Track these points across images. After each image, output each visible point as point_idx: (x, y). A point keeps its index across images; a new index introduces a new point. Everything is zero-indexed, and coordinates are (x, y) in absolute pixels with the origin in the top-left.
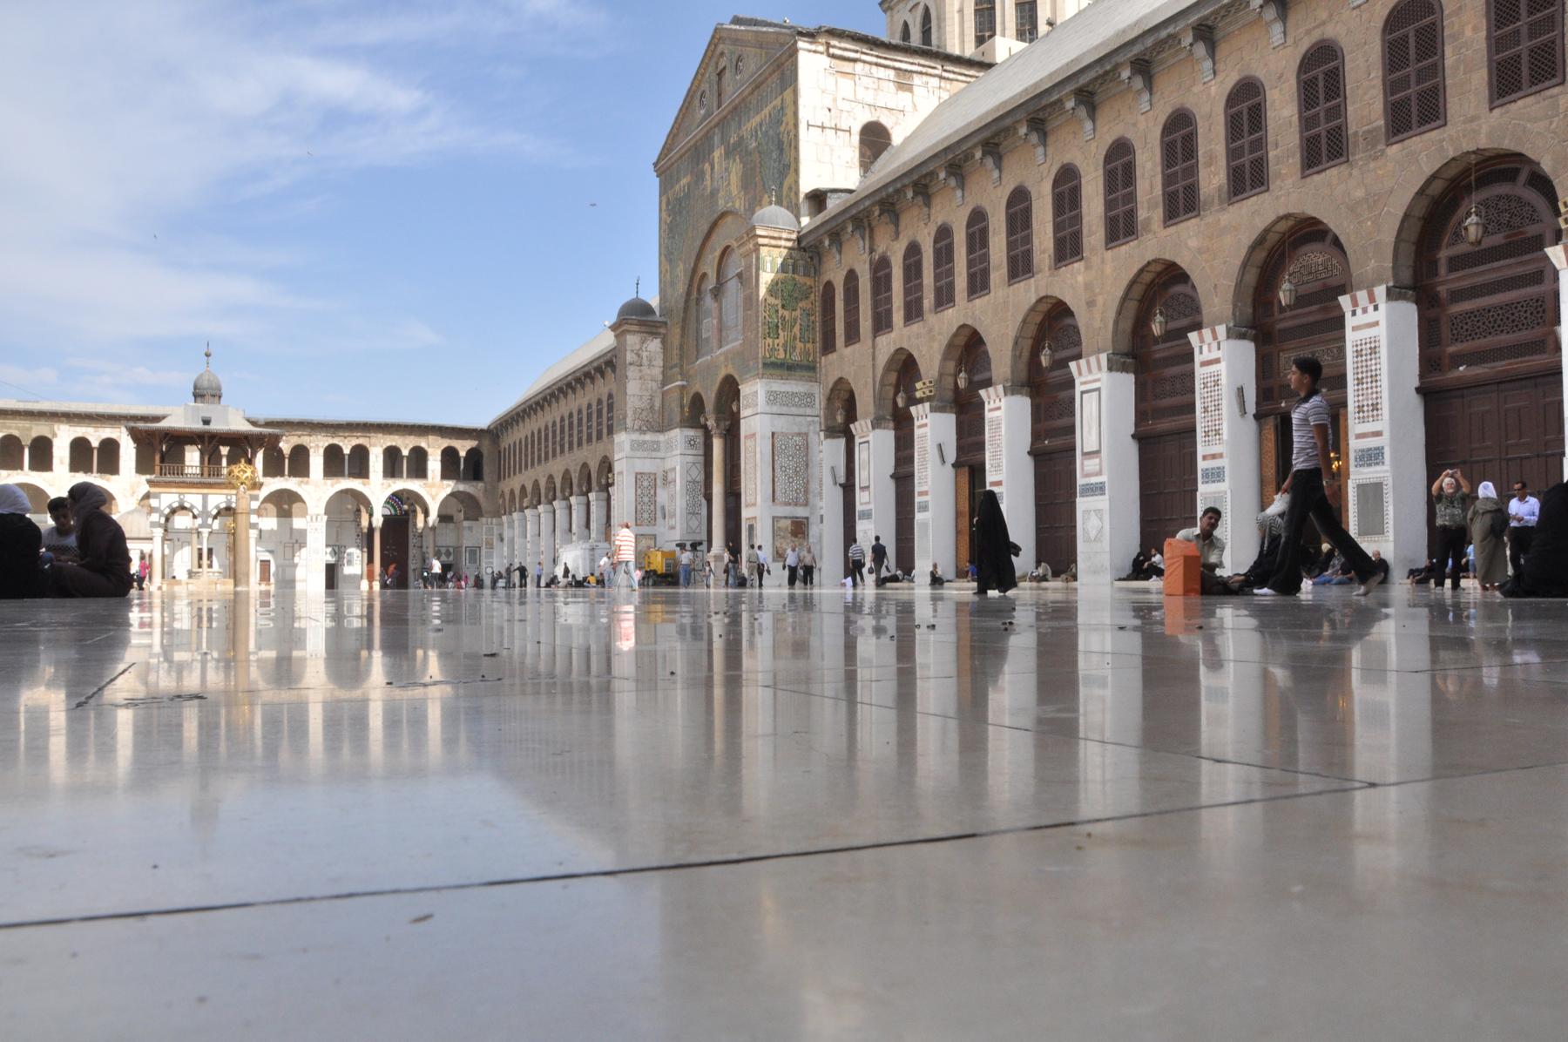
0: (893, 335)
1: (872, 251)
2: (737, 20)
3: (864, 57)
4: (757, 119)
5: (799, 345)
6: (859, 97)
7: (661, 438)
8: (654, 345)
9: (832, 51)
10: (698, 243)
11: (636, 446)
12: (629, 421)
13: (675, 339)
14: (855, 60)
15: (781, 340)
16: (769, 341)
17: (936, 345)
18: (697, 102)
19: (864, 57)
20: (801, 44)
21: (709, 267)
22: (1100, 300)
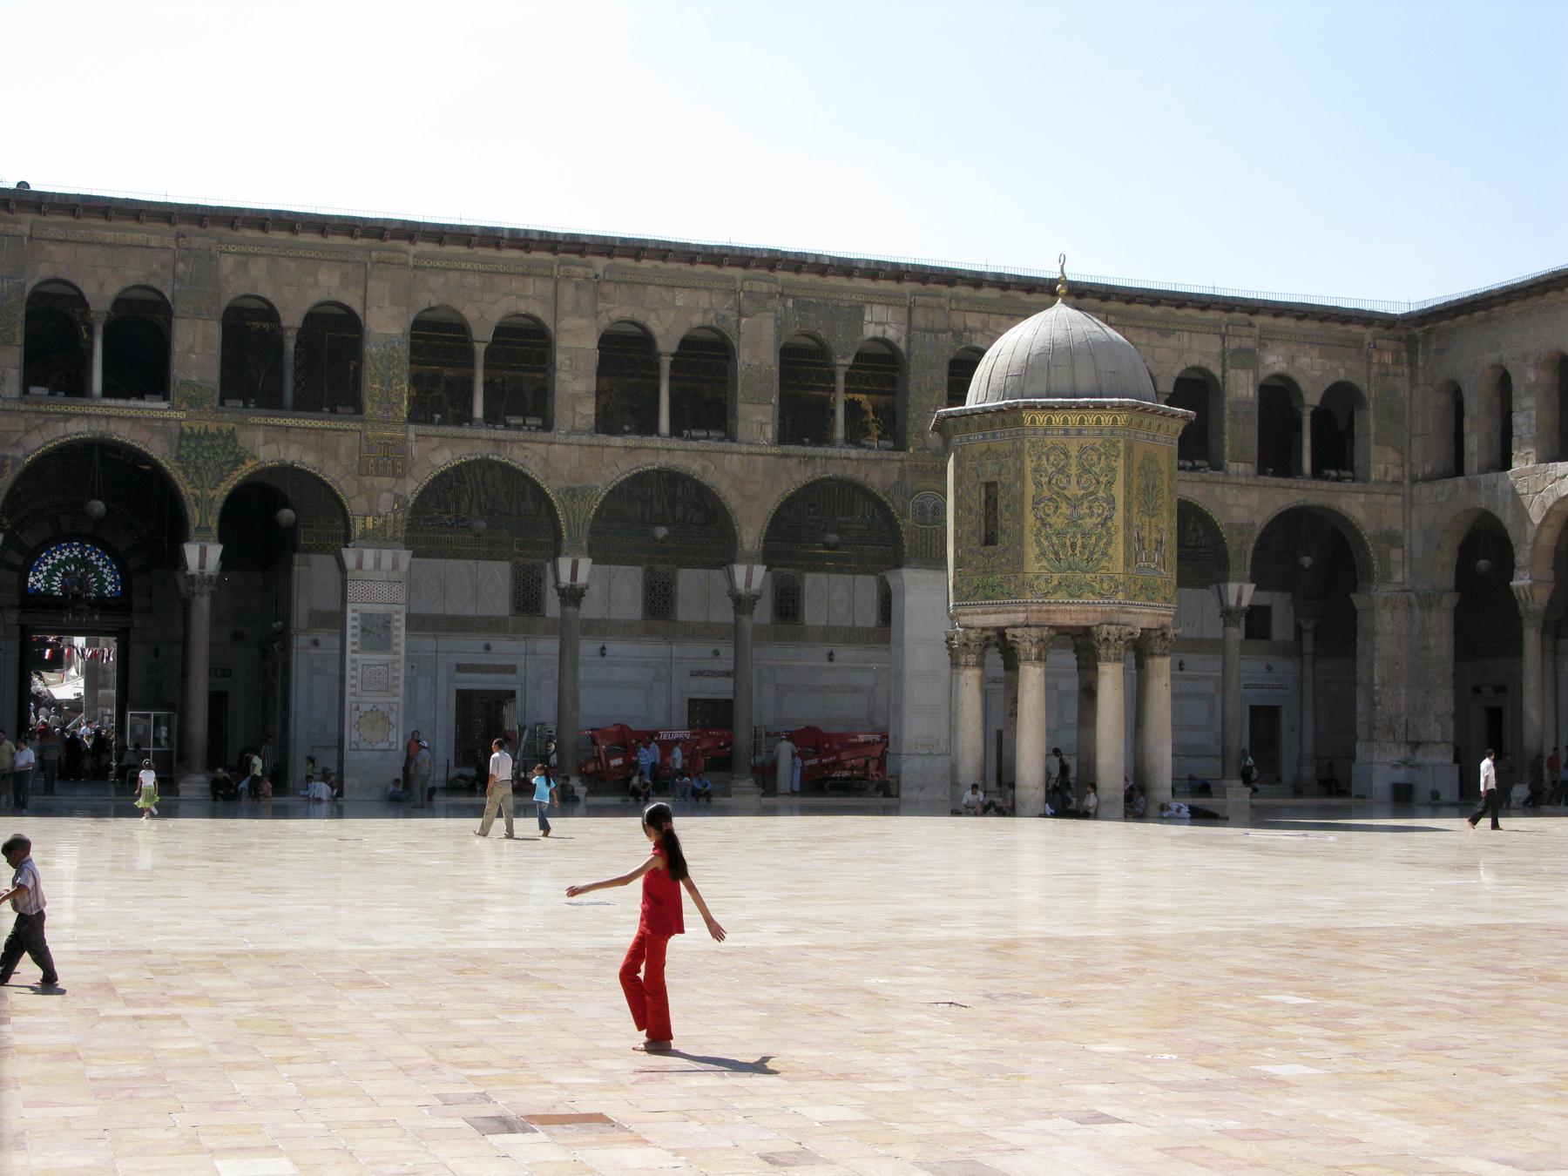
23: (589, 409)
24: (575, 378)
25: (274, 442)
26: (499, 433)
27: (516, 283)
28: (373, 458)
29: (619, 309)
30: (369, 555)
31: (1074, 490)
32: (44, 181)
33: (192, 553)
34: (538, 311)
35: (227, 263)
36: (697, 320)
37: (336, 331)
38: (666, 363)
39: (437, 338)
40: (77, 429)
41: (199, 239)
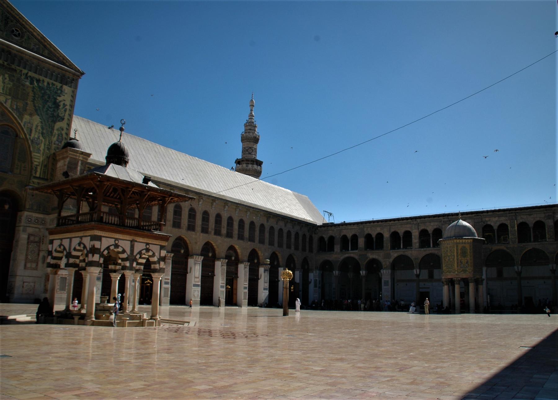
4: (36, 76)
22: (198, 243)
23: (418, 244)
24: (415, 240)
25: (371, 255)
26: (404, 250)
27: (406, 226)
28: (386, 256)
29: (422, 227)
30: (385, 271)
31: (449, 254)
32: (348, 220)
33: (361, 272)
34: (409, 229)
35: (365, 229)
36: (435, 227)
37: (380, 236)
38: (431, 235)
39: (395, 235)
40: (347, 255)
41: (361, 226)
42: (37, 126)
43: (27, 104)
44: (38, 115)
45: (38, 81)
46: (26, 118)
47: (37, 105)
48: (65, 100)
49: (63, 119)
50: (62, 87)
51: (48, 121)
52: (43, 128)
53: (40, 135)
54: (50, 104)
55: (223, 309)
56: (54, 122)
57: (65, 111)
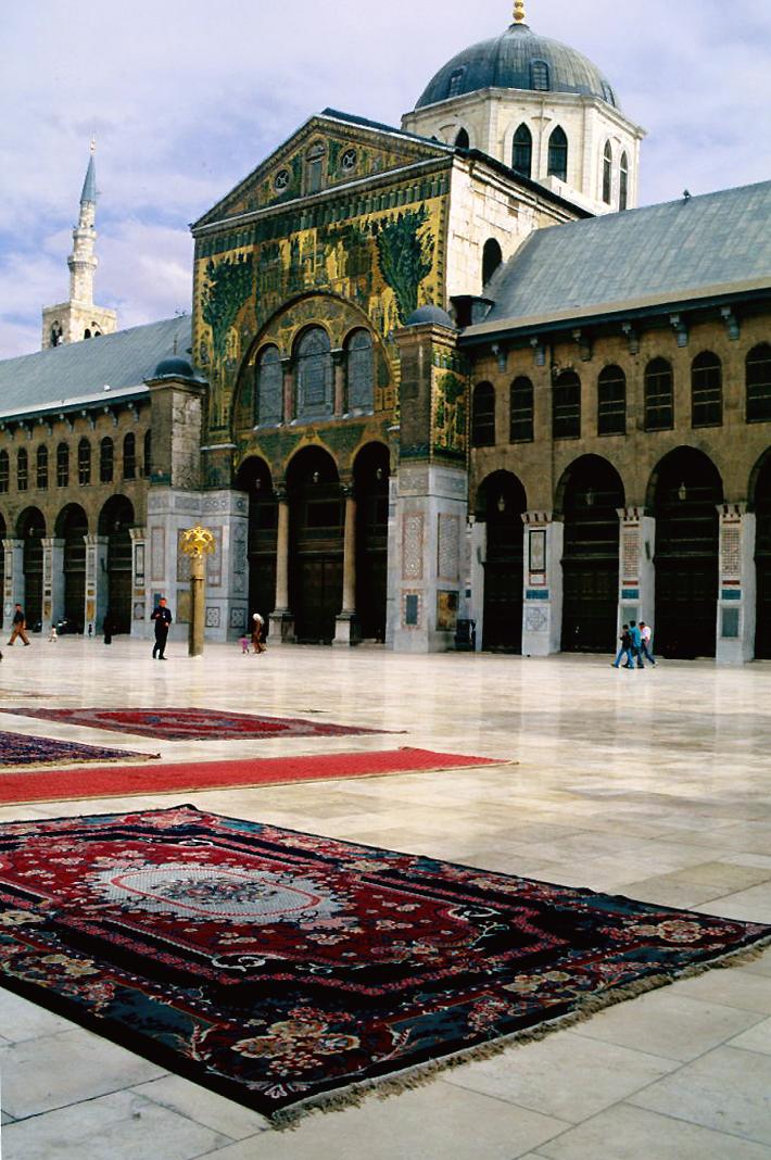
0: (581, 442)
1: (552, 364)
2: (328, 112)
3: (493, 182)
4: (380, 215)
5: (456, 435)
6: (486, 217)
7: (200, 496)
8: (195, 404)
9: (475, 172)
10: (264, 316)
11: (181, 504)
12: (173, 478)
13: (224, 399)
14: (487, 183)
15: (444, 430)
16: (438, 429)
17: (644, 459)
18: (270, 179)
19: (493, 182)
20: (455, 162)
21: (282, 338)
42: (390, 307)
43: (371, 275)
44: (390, 285)
45: (384, 222)
46: (374, 299)
47: (385, 267)
48: (429, 229)
49: (429, 268)
50: (422, 206)
51: (406, 288)
52: (399, 307)
53: (398, 322)
54: (404, 252)
55: (636, 670)
56: (415, 284)
57: (432, 249)
